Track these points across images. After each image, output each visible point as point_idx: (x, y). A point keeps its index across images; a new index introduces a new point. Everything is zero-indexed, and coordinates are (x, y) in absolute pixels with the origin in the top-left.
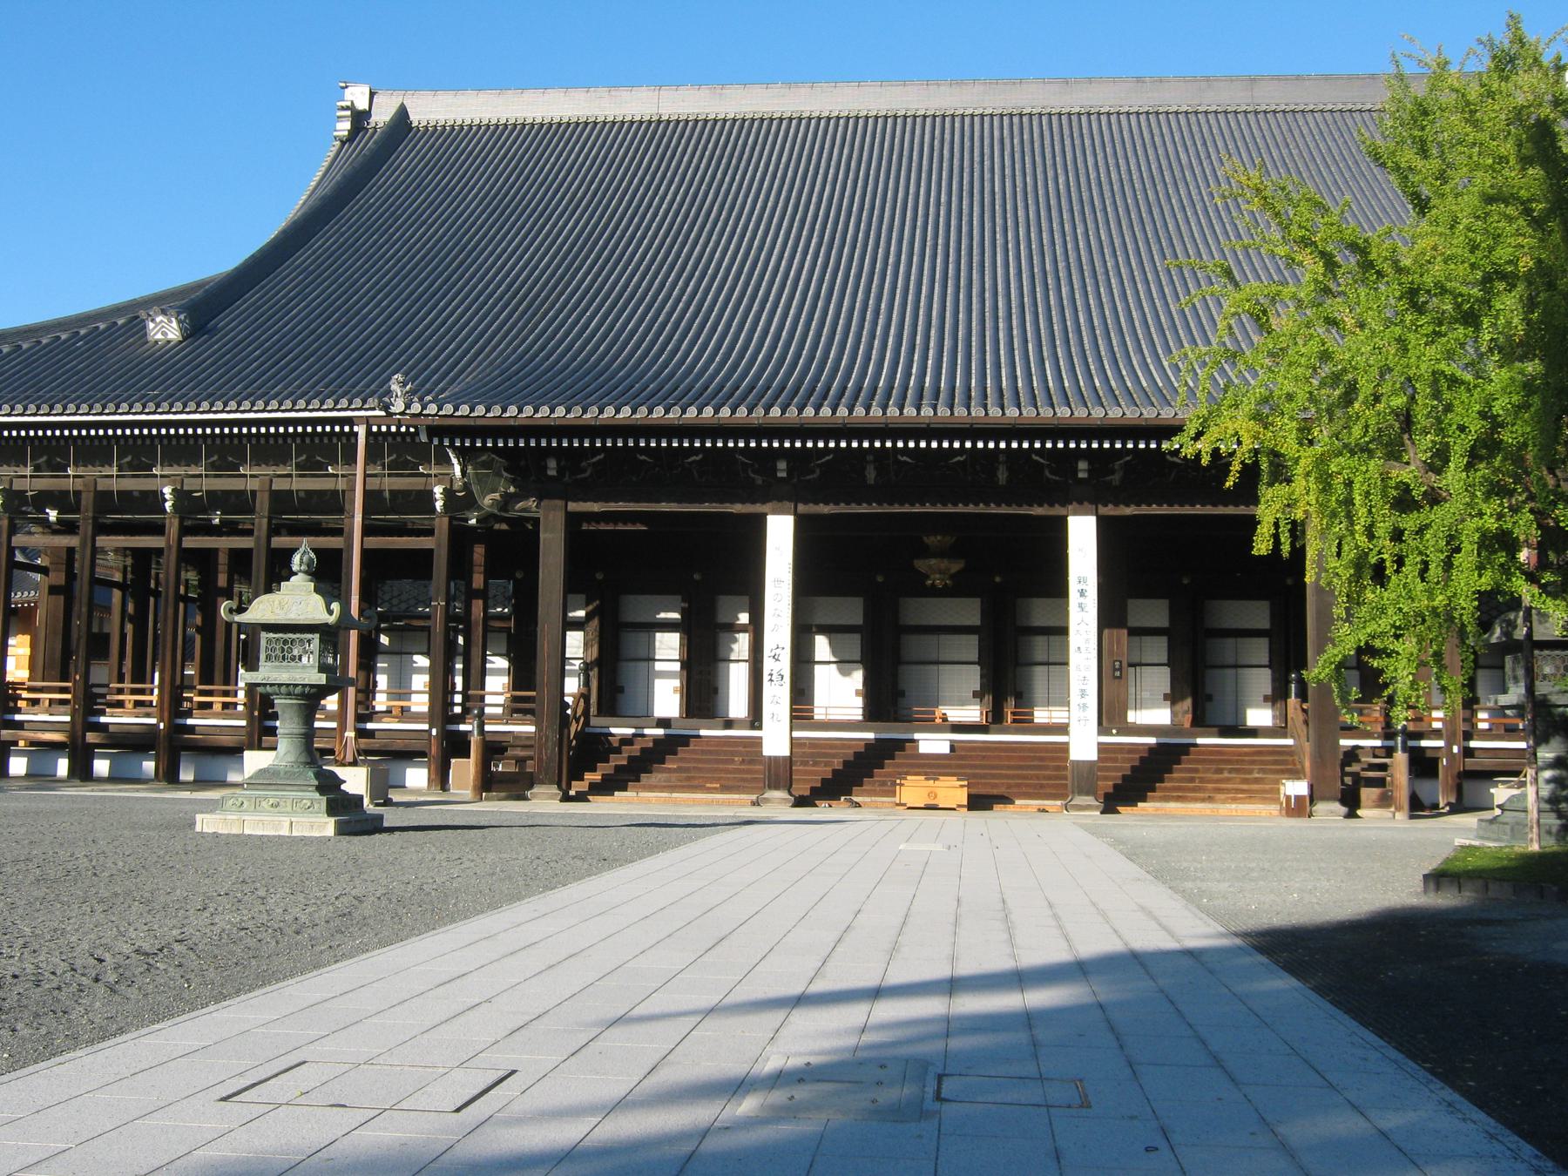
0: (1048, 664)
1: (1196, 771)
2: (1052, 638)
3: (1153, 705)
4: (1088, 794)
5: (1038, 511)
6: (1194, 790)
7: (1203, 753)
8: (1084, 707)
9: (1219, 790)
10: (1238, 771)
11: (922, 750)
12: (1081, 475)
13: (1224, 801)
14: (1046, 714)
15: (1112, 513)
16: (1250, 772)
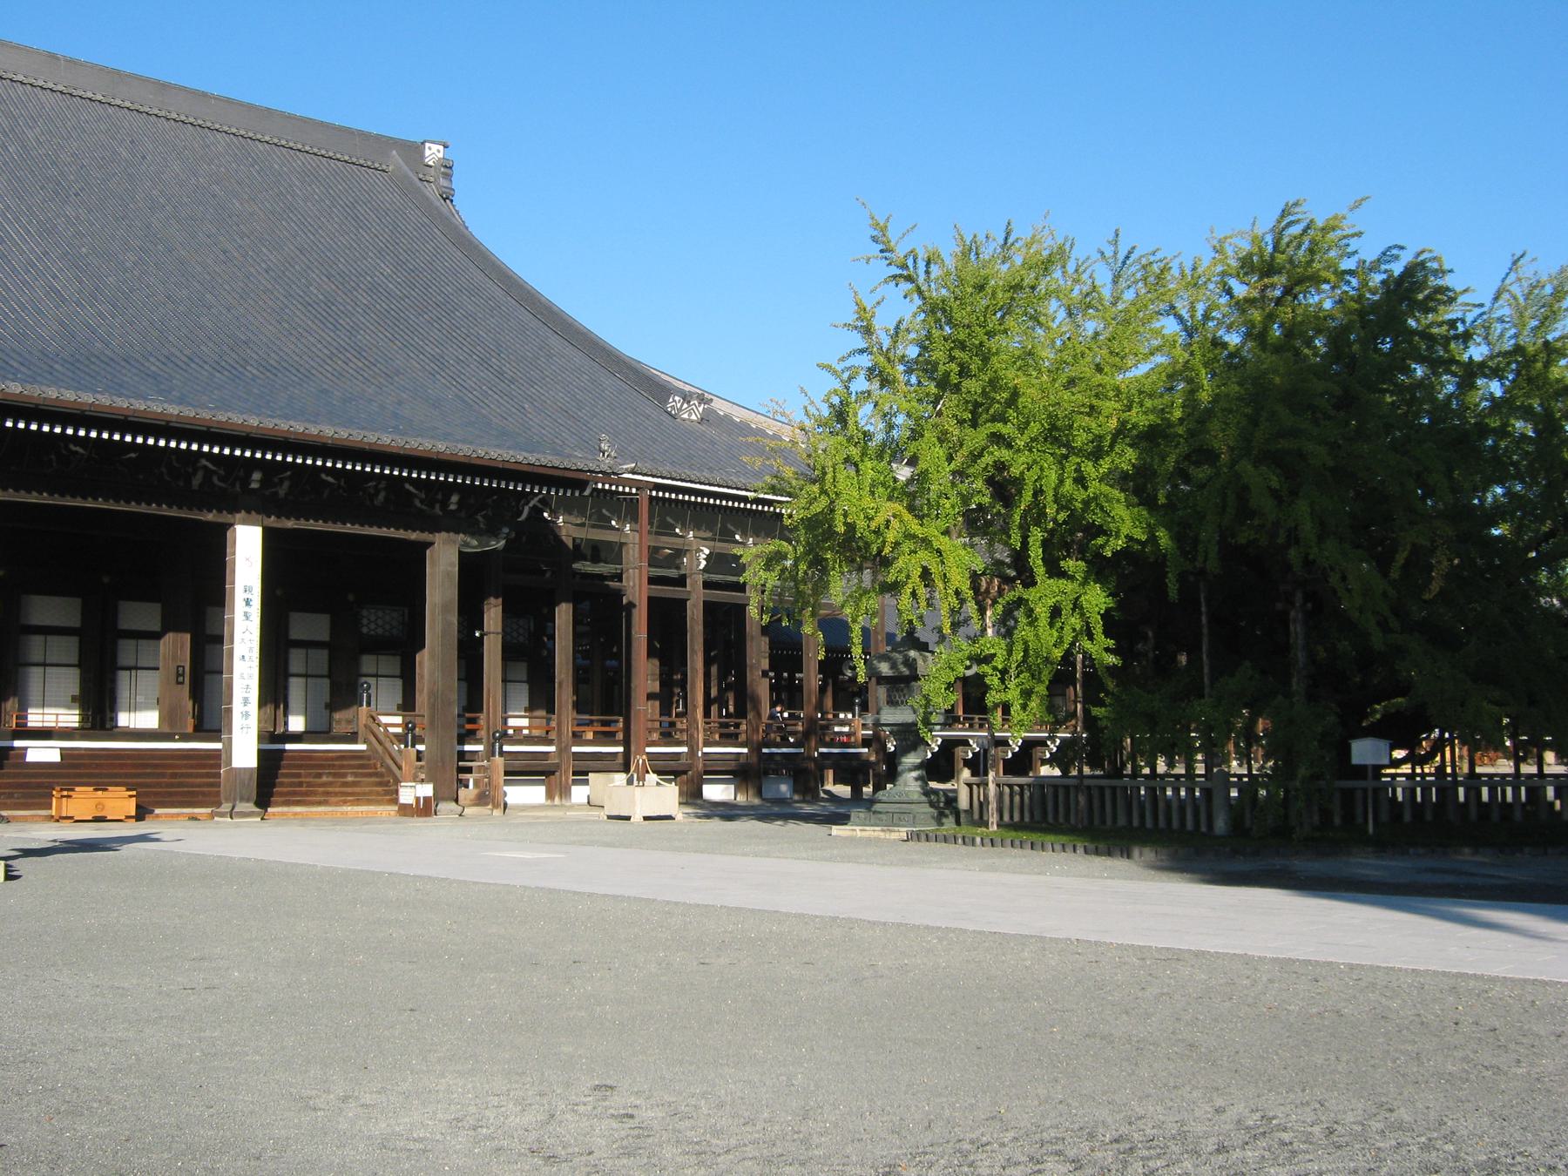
0: (45, 665)
1: (299, 775)
2: (49, 638)
3: (147, 707)
4: (248, 801)
5: (210, 517)
6: (306, 794)
7: (293, 758)
8: (246, 715)
9: (328, 794)
10: (335, 775)
11: (29, 759)
12: (254, 485)
13: (337, 804)
14: (40, 718)
15: (279, 525)
16: (344, 775)
